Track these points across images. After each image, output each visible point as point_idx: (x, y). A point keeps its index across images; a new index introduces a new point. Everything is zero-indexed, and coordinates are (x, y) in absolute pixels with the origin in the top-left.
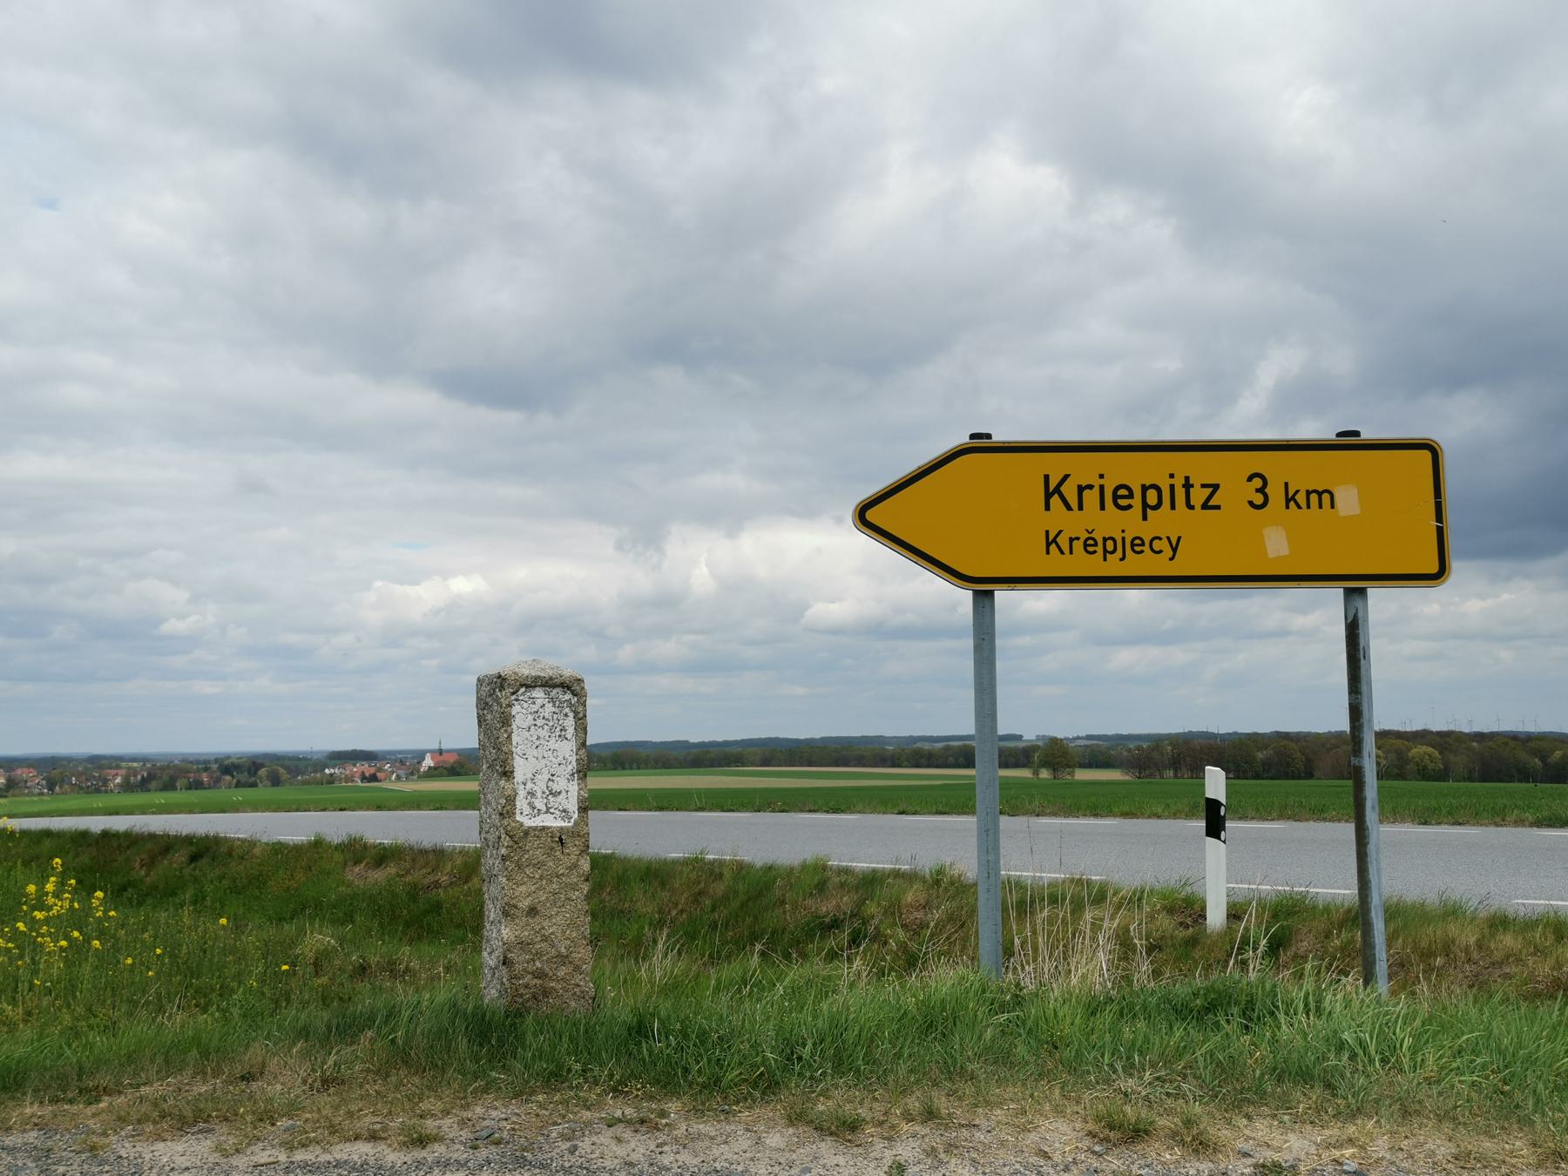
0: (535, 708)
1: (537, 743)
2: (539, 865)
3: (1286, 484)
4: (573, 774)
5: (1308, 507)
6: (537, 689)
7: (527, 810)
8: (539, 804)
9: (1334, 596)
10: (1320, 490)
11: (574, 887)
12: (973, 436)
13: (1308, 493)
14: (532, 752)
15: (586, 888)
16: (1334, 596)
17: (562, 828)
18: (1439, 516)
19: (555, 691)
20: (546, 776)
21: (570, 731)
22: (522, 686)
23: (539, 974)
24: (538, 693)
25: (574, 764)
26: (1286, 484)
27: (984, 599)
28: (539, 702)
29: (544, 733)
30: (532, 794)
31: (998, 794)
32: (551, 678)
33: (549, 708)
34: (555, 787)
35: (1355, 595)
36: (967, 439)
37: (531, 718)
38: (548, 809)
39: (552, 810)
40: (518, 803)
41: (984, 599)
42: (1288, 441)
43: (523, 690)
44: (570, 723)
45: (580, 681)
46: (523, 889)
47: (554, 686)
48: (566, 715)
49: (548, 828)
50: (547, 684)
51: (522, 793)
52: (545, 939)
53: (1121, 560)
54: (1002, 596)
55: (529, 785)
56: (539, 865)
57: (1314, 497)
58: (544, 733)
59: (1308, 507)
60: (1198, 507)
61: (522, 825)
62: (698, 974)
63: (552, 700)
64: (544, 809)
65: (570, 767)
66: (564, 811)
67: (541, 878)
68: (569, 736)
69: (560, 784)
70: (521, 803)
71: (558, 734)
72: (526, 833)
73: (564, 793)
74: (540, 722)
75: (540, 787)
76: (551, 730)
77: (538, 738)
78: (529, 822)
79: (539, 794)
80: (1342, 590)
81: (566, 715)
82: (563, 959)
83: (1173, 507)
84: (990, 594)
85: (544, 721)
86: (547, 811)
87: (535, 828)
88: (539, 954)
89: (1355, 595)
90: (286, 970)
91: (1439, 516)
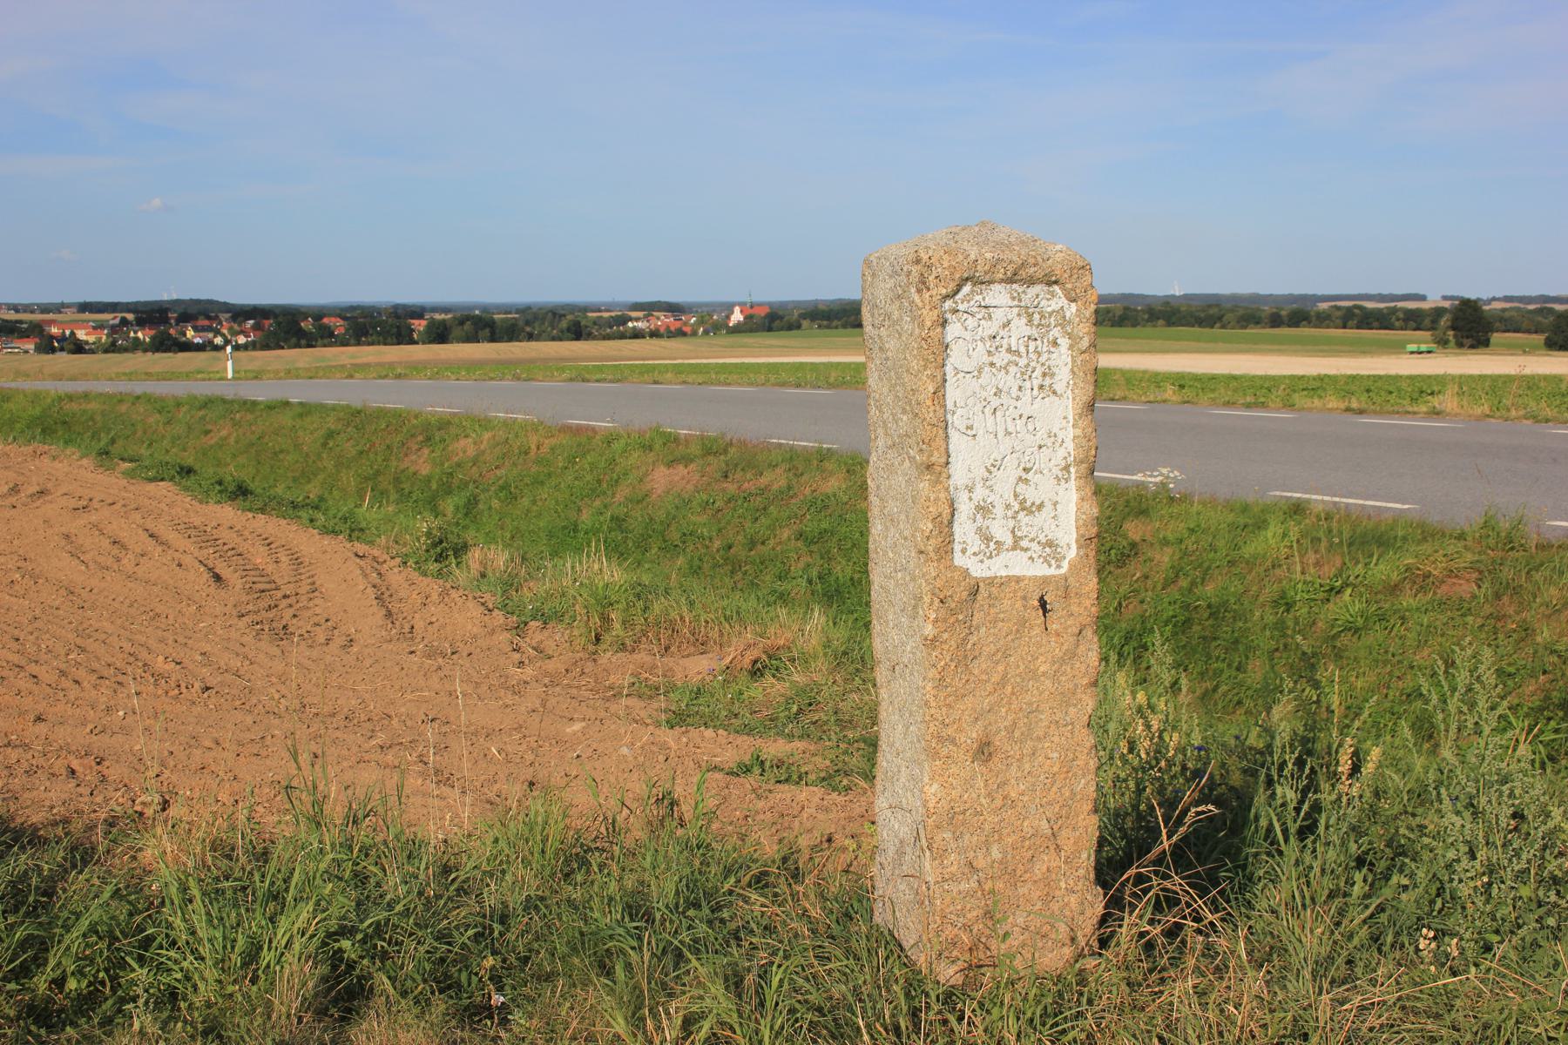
0: (990, 328)
1: (995, 402)
4: (1066, 468)
6: (996, 287)
7: (975, 544)
8: (1000, 531)
17: (1045, 580)
20: (1010, 472)
24: (998, 295)
25: (1070, 445)
28: (999, 315)
33: (1020, 328)
34: (1031, 495)
39: (1024, 543)
47: (1031, 282)
48: (1055, 344)
49: (1018, 580)
51: (965, 508)
58: (1009, 381)
61: (966, 573)
64: (1009, 541)
65: (1061, 453)
66: (1050, 544)
68: (1059, 387)
69: (1041, 488)
70: (964, 529)
71: (1036, 383)
73: (1048, 507)
76: (1026, 373)
77: (998, 393)
78: (978, 570)
79: (999, 511)
85: (1009, 357)
86: (1014, 548)
87: (991, 581)
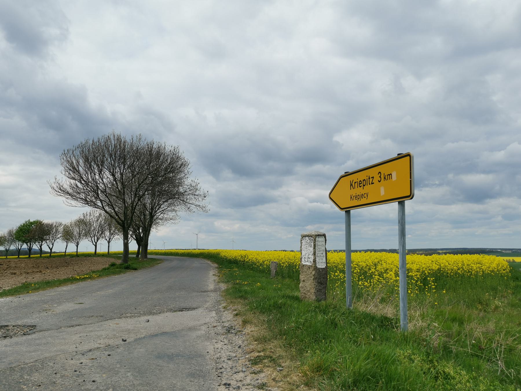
0: (306, 241)
2: (306, 272)
3: (384, 174)
5: (388, 180)
7: (304, 261)
8: (306, 260)
9: (395, 205)
10: (381, 176)
11: (311, 277)
12: (345, 173)
13: (388, 175)
14: (305, 250)
15: (313, 277)
16: (395, 205)
17: (309, 265)
18: (411, 178)
19: (310, 237)
20: (308, 254)
21: (313, 245)
22: (304, 236)
23: (305, 294)
24: (307, 238)
26: (384, 174)
27: (348, 213)
28: (307, 240)
29: (308, 246)
30: (305, 258)
31: (174, 257)
32: (309, 235)
34: (309, 257)
35: (402, 204)
36: (344, 173)
37: (305, 243)
38: (308, 261)
40: (302, 260)
41: (348, 213)
42: (384, 161)
43: (304, 237)
44: (312, 244)
45: (325, 234)
46: (302, 276)
47: (310, 236)
48: (312, 242)
49: (307, 265)
50: (308, 236)
51: (303, 258)
52: (306, 287)
53: (367, 199)
54: (352, 212)
55: (305, 256)
56: (306, 272)
57: (389, 176)
58: (308, 246)
59: (388, 180)
60: (371, 184)
62: (499, 320)
63: (309, 239)
66: (311, 262)
67: (306, 275)
68: (312, 247)
69: (310, 256)
70: (303, 260)
72: (303, 266)
74: (307, 244)
75: (306, 257)
76: (309, 245)
77: (307, 247)
78: (304, 263)
79: (306, 258)
80: (398, 202)
81: (312, 242)
82: (309, 291)
83: (367, 185)
84: (349, 211)
86: (307, 262)
87: (305, 265)
88: (305, 289)
89: (402, 204)
90: (436, 304)
91: (411, 178)
